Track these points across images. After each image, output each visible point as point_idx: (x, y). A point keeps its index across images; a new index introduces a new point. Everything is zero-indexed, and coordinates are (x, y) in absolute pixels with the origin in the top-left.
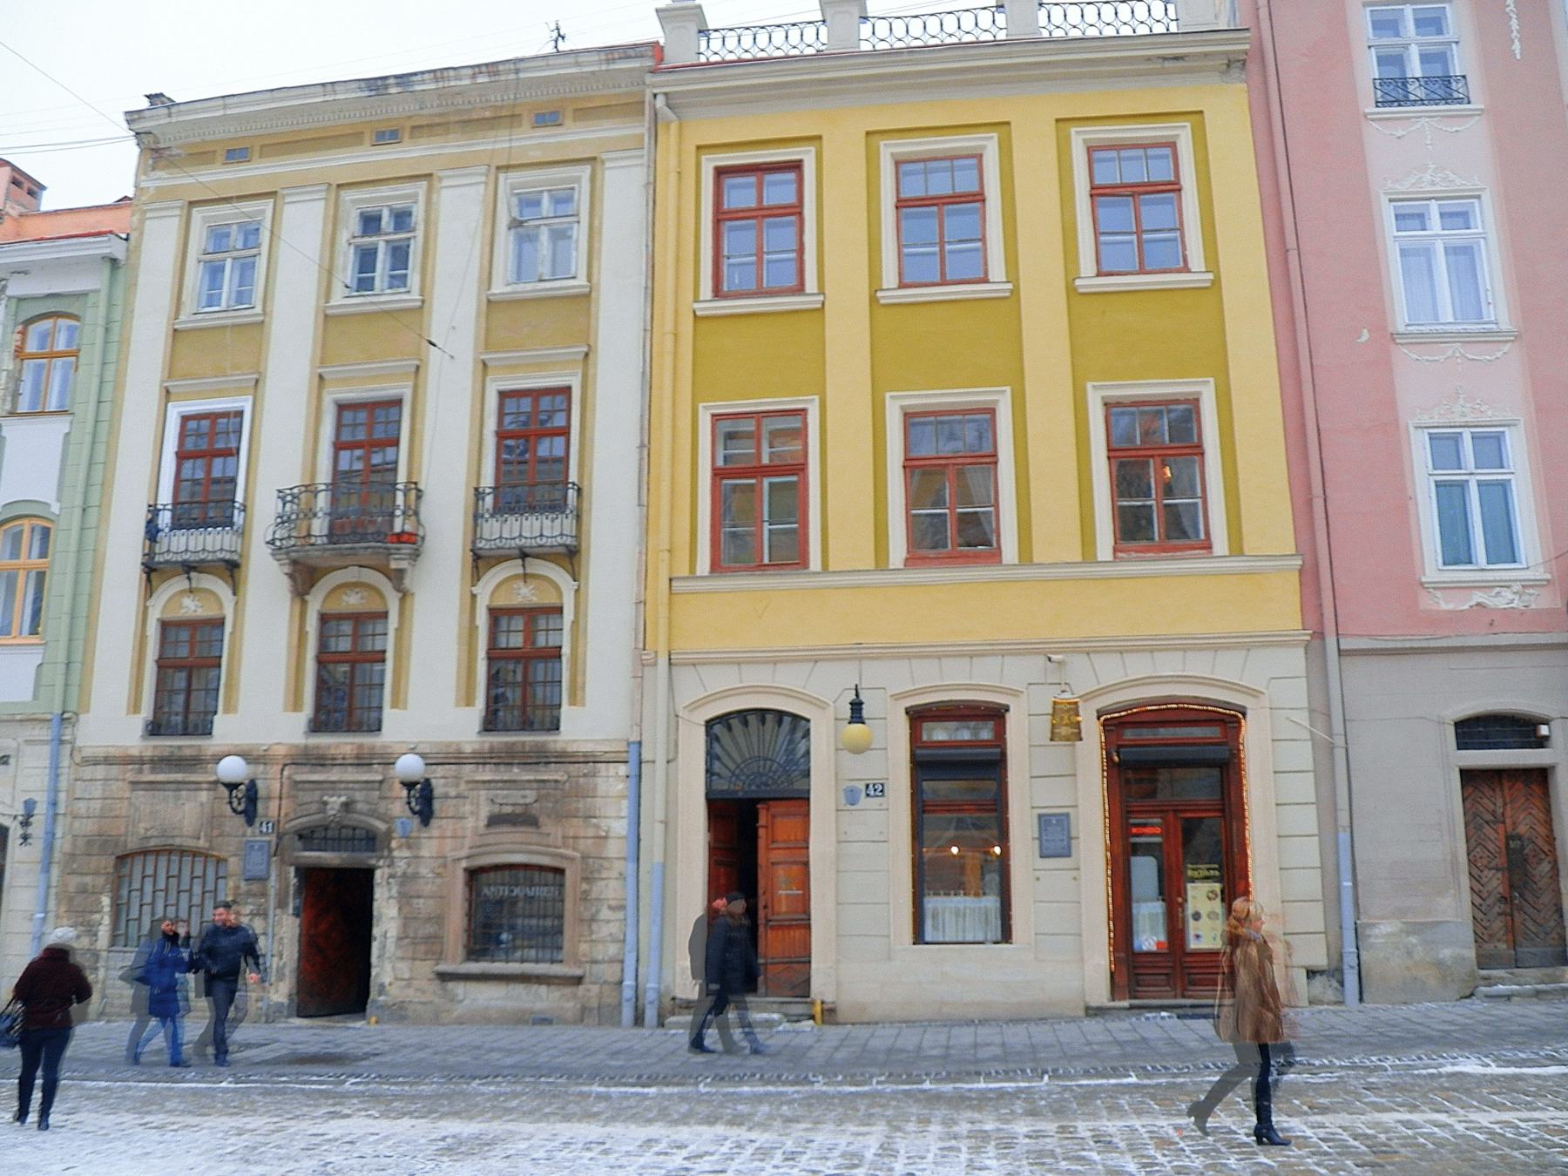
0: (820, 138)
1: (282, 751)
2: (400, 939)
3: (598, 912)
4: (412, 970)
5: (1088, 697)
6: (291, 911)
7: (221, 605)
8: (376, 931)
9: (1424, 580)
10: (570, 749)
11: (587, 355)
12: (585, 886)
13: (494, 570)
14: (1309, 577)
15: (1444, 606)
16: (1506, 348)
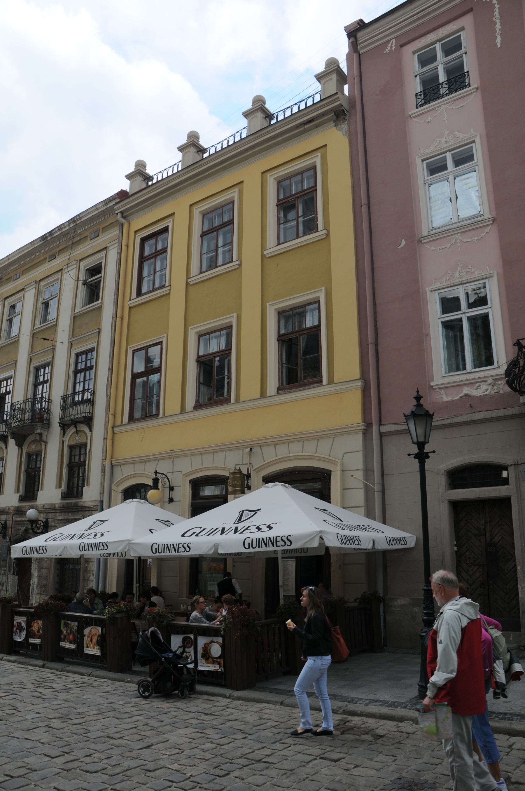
0: (173, 214)
1: (12, 509)
2: (38, 585)
3: (90, 576)
4: (40, 599)
5: (258, 470)
6: (12, 573)
7: (3, 453)
8: (31, 582)
9: (432, 384)
10: (85, 505)
11: (99, 333)
12: (86, 565)
13: (69, 430)
14: (365, 390)
15: (445, 399)
16: (487, 230)
